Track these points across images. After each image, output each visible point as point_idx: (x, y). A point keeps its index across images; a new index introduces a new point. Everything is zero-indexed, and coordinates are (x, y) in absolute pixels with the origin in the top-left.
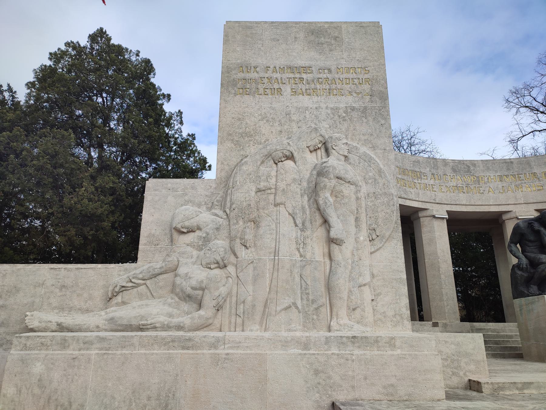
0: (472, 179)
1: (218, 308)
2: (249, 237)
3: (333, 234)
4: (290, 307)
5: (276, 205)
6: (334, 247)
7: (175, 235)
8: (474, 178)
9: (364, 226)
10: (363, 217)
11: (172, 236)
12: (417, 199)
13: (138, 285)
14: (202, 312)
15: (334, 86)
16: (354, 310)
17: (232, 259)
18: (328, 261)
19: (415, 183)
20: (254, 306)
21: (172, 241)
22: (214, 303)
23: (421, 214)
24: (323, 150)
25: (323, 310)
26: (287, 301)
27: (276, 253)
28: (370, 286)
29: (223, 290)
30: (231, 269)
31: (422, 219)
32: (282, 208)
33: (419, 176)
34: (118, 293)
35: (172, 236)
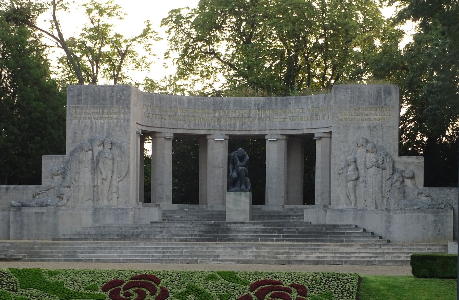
1: (68, 200)
2: (76, 178)
3: (103, 178)
4: (89, 200)
5: (85, 167)
6: (104, 181)
7: (54, 176)
9: (115, 173)
10: (115, 170)
11: (52, 176)
13: (42, 193)
14: (63, 201)
15: (110, 116)
16: (110, 200)
17: (72, 185)
18: (102, 185)
20: (78, 199)
21: (52, 178)
22: (67, 199)
23: (208, 137)
24: (102, 146)
25: (100, 200)
26: (88, 198)
27: (85, 183)
28: (117, 193)
29: (69, 194)
30: (72, 188)
31: (209, 141)
32: (87, 169)
34: (37, 195)
35: (52, 176)
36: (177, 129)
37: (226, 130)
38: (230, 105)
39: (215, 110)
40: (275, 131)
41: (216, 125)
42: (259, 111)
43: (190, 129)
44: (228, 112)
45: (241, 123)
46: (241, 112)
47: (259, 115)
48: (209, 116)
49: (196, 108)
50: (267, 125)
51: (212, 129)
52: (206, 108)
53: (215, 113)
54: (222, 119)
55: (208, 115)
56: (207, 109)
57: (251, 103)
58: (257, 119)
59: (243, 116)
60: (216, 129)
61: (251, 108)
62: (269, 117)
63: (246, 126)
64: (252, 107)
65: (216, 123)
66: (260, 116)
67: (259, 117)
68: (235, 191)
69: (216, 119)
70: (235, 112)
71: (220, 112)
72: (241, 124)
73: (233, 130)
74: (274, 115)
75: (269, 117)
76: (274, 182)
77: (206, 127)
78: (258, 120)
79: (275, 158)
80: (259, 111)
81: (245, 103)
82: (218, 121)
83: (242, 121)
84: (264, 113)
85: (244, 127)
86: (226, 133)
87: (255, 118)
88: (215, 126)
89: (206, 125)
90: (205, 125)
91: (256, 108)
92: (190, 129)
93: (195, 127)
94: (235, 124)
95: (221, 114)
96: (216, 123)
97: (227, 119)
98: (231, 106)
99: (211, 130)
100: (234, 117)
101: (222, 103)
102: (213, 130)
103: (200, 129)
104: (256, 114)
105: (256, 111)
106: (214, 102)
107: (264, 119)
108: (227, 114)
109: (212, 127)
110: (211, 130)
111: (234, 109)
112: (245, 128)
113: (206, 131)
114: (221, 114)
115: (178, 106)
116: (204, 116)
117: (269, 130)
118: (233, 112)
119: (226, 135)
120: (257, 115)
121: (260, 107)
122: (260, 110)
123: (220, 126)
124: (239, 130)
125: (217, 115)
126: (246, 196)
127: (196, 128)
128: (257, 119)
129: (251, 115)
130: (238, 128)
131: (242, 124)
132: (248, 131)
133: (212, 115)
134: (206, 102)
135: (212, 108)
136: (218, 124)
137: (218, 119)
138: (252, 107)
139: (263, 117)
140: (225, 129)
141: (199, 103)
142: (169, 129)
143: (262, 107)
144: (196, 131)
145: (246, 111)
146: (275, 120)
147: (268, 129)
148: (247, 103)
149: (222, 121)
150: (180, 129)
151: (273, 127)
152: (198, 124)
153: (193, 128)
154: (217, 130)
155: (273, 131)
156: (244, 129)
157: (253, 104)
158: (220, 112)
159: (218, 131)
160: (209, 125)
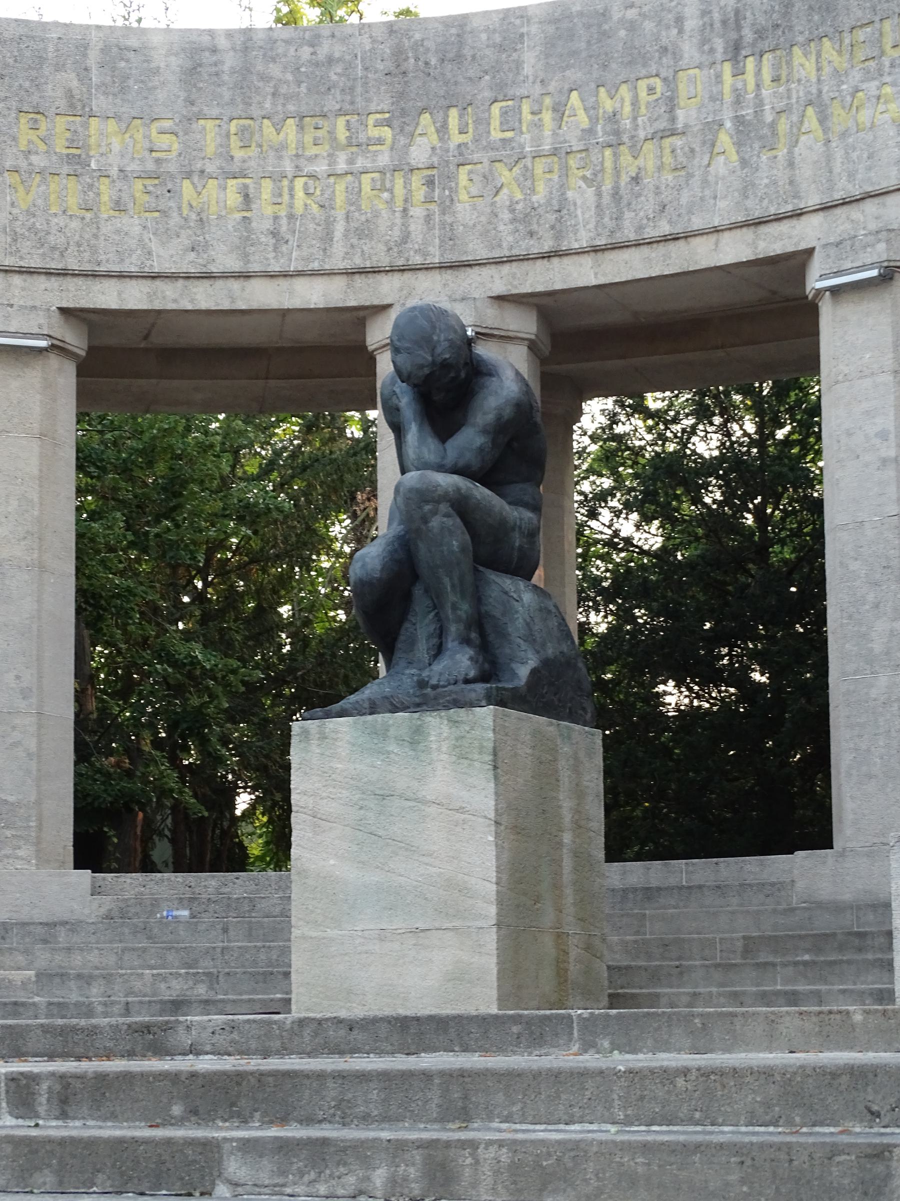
0: (643, 94)
8: (651, 90)
12: (316, 265)
19: (311, 182)
33: (342, 134)
36: (94, 275)
37: (499, 262)
38: (519, 65)
39: (404, 113)
40: (870, 207)
41: (416, 228)
42: (739, 72)
43: (208, 276)
44: (510, 120)
45: (607, 186)
46: (608, 105)
47: (738, 100)
48: (360, 163)
49: (256, 112)
50: (805, 172)
51: (384, 261)
52: (331, 104)
53: (403, 140)
54: (463, 174)
55: (351, 161)
56: (341, 113)
57: (679, 20)
58: (725, 140)
59: (617, 133)
60: (417, 260)
61: (677, 56)
62: (816, 102)
63: (648, 205)
64: (689, 50)
65: (417, 212)
66: (748, 112)
67: (739, 120)
68: (373, 709)
69: (417, 180)
70: (559, 110)
71: (442, 130)
72: (606, 199)
73: (547, 256)
74: (856, 75)
75: (816, 102)
76: (877, 647)
77: (338, 248)
78: (739, 144)
79: (883, 435)
80: (739, 72)
81: (632, 27)
82: (429, 200)
83: (617, 171)
84: (776, 80)
85: (628, 215)
86: (500, 288)
87: (714, 126)
88: (406, 237)
89: (339, 229)
90: (328, 238)
91: (719, 44)
92: (208, 276)
93: (245, 257)
94: (561, 207)
95: (456, 139)
96: (417, 212)
97: (505, 175)
98: (527, 70)
99: (376, 271)
100: (554, 153)
101: (459, 58)
102: (392, 271)
103: (285, 275)
104: (716, 98)
105: (719, 78)
106: (399, 54)
107: (783, 126)
108: (496, 135)
109: (382, 247)
110: (376, 271)
111: (552, 87)
112: (640, 228)
113: (340, 282)
114: (456, 139)
115: (99, 103)
116: (321, 168)
117: (825, 208)
118: (547, 117)
119: (500, 299)
120: (728, 97)
121: (748, 34)
122: (750, 63)
123: (450, 237)
124: (596, 250)
125: (419, 154)
126: (461, 754)
127: (255, 267)
128: (725, 140)
129: (680, 114)
130: (583, 239)
131: (616, 194)
132: (661, 249)
133: (384, 159)
134: (330, 61)
135: (382, 102)
136: (428, 218)
137: (430, 183)
138: (689, 50)
139: (769, 117)
140: (483, 253)
141: (275, 70)
142: (17, 280)
143: (760, 34)
144: (256, 285)
145: (643, 94)
146: (864, 116)
147: (814, 200)
148: (649, 26)
149: (463, 196)
150: (121, 276)
151: (851, 176)
152: (275, 234)
153: (233, 264)
154: (428, 269)
155: (855, 213)
156: (630, 234)
157: (692, 24)
158: (442, 130)
159: (436, 276)
160: (364, 231)
